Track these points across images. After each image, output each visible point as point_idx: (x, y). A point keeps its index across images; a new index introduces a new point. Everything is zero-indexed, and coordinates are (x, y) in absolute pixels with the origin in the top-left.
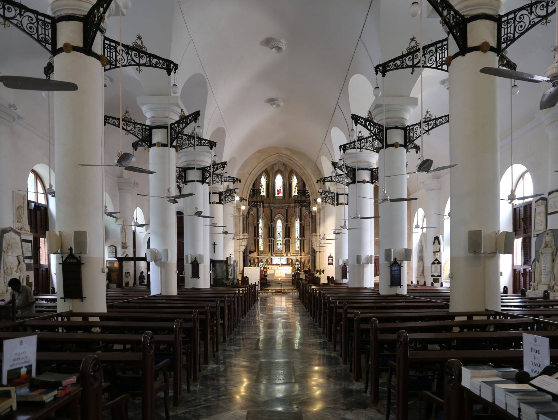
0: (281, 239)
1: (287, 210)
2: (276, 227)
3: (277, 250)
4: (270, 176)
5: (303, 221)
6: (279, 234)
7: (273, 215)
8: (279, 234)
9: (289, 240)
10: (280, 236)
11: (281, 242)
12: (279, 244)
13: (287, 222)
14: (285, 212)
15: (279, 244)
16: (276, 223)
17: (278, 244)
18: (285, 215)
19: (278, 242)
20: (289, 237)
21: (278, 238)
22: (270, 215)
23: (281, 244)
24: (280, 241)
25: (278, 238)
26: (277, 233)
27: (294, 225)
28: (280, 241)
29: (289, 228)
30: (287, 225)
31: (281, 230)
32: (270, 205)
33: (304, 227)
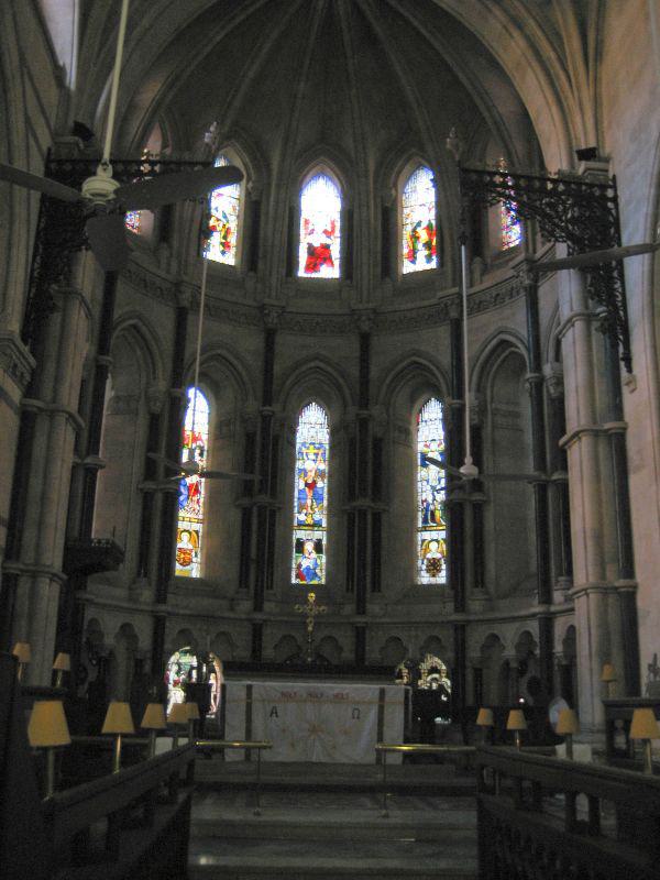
0: (321, 516)
1: (365, 340)
2: (293, 445)
3: (294, 581)
4: (268, 166)
6: (311, 486)
7: (277, 369)
8: (311, 486)
10: (317, 498)
11: (320, 535)
12: (309, 547)
15: (309, 547)
17: (300, 546)
19: (299, 534)
21: (302, 507)
22: (257, 364)
23: (318, 547)
24: (317, 525)
25: (302, 507)
26: (300, 484)
28: (317, 525)
31: (323, 466)
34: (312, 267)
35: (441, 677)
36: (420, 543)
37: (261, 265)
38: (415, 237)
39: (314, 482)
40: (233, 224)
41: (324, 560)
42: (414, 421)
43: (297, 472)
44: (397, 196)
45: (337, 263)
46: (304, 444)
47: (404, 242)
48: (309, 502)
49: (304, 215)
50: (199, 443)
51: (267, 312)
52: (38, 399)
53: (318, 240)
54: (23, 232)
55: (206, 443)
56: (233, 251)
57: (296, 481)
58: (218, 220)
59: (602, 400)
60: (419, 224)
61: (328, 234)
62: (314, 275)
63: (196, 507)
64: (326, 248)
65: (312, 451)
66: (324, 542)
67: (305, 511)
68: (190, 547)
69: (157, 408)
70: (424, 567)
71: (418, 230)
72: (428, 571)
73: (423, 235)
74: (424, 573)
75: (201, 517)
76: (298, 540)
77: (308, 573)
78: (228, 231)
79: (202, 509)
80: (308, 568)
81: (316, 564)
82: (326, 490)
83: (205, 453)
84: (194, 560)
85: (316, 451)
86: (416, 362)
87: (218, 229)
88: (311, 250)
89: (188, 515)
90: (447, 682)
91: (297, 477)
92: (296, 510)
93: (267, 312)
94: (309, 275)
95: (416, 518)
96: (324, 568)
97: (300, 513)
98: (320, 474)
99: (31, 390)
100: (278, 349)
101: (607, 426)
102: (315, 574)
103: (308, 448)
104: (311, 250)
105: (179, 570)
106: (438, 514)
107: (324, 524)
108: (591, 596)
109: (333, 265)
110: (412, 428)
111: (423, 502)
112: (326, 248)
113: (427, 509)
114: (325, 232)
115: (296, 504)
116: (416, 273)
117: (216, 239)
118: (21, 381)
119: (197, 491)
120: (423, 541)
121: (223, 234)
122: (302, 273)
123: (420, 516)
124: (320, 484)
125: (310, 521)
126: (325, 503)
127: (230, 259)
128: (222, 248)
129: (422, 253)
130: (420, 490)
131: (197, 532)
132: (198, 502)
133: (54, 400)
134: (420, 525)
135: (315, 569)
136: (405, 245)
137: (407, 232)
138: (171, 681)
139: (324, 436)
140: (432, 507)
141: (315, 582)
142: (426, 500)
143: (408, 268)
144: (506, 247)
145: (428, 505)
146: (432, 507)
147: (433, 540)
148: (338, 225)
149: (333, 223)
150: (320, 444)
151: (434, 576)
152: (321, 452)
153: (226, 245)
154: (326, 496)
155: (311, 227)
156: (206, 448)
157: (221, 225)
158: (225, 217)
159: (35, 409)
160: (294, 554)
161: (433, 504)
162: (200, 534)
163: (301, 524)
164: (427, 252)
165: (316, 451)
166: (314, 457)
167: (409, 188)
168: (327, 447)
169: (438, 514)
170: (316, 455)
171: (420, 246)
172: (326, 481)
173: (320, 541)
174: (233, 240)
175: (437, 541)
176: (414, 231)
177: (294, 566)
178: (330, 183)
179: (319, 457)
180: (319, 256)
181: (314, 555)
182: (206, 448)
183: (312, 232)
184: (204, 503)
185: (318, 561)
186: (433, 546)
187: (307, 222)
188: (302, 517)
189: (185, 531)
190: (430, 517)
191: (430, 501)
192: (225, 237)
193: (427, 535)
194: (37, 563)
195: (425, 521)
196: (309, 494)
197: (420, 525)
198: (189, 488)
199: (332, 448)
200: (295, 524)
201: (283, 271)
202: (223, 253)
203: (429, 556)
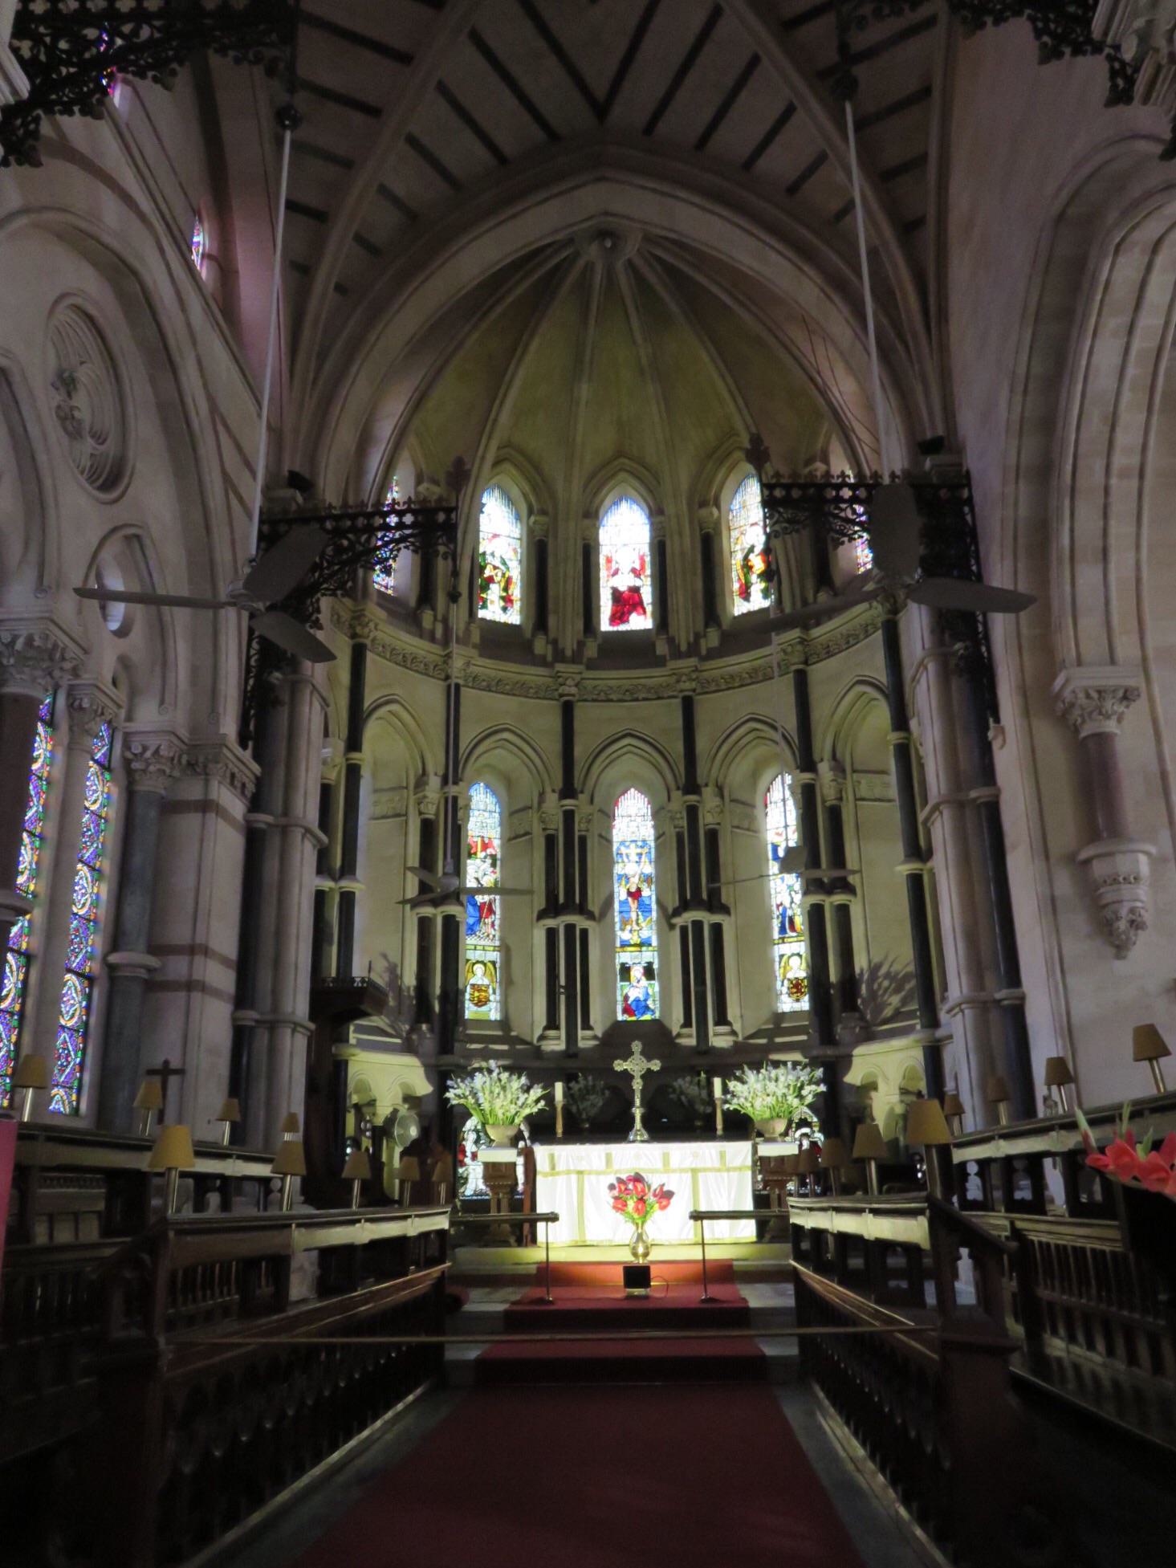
1: (688, 706)
3: (620, 1017)
6: (636, 895)
7: (578, 751)
8: (636, 895)
9: (717, 929)
10: (644, 909)
11: (650, 955)
12: (637, 972)
13: (691, 786)
14: (678, 722)
15: (637, 972)
16: (608, 816)
17: (625, 971)
18: (678, 748)
19: (624, 957)
20: (715, 904)
21: (625, 922)
22: (552, 747)
23: (649, 972)
24: (643, 944)
25: (625, 922)
26: (621, 893)
27: (752, 818)
28: (643, 944)
29: (713, 836)
30: (692, 812)
31: (649, 869)
32: (556, 677)
33: (835, 814)
34: (619, 616)
35: (813, 1132)
36: (777, 959)
37: (552, 621)
38: (747, 567)
39: (639, 890)
40: (515, 572)
41: (657, 989)
42: (759, 803)
43: (615, 878)
44: (719, 518)
45: (649, 609)
46: (622, 843)
47: (734, 575)
48: (633, 916)
49: (604, 552)
50: (489, 851)
53: (624, 582)
55: (498, 850)
56: (517, 605)
57: (616, 890)
58: (495, 568)
59: (967, 761)
60: (751, 550)
61: (637, 573)
62: (623, 627)
64: (635, 590)
65: (633, 851)
66: (656, 966)
67: (628, 927)
68: (486, 981)
69: (430, 812)
70: (785, 990)
71: (752, 557)
72: (790, 994)
73: (758, 564)
74: (785, 998)
75: (497, 943)
76: (623, 965)
77: (637, 1006)
78: (508, 581)
79: (498, 935)
80: (637, 1000)
81: (648, 994)
82: (654, 898)
83: (498, 863)
84: (492, 998)
85: (639, 851)
87: (497, 579)
88: (617, 595)
89: (482, 942)
90: (819, 1137)
91: (616, 886)
92: (617, 926)
94: (615, 629)
95: (769, 928)
96: (657, 998)
97: (622, 929)
98: (647, 879)
100: (578, 725)
101: (973, 794)
102: (647, 1008)
103: (628, 847)
104: (617, 595)
105: (470, 1011)
106: (799, 921)
107: (654, 943)
108: (966, 1011)
109: (645, 612)
110: (759, 811)
111: (778, 906)
112: (635, 590)
113: (783, 915)
114: (634, 571)
115: (617, 919)
116: (750, 614)
117: (494, 593)
119: (491, 911)
120: (781, 956)
121: (503, 584)
122: (605, 626)
123: (776, 924)
124: (646, 892)
125: (635, 940)
126: (654, 914)
127: (514, 617)
128: (502, 603)
129: (757, 587)
130: (773, 892)
131: (494, 963)
132: (493, 925)
134: (776, 935)
135: (646, 1000)
136: (735, 578)
137: (737, 561)
138: (468, 1154)
139: (647, 831)
140: (789, 913)
141: (647, 1017)
142: (781, 904)
143: (740, 608)
144: (862, 570)
145: (785, 910)
146: (789, 913)
147: (793, 955)
148: (648, 559)
149: (642, 559)
150: (644, 841)
151: (798, 1000)
152: (646, 850)
153: (507, 600)
154: (654, 906)
155: (614, 566)
156: (499, 856)
157: (500, 574)
158: (504, 563)
160: (619, 984)
161: (791, 907)
162: (498, 965)
163: (625, 945)
164: (763, 585)
165: (639, 851)
166: (637, 859)
167: (736, 505)
168: (653, 844)
169: (799, 921)
170: (640, 855)
171: (754, 578)
172: (653, 887)
173: (650, 964)
174: (516, 592)
175: (799, 955)
176: (746, 558)
177: (619, 998)
178: (635, 507)
179: (643, 856)
180: (626, 603)
181: (644, 982)
182: (499, 856)
183: (616, 573)
184: (500, 926)
185: (650, 992)
186: (795, 961)
187: (609, 561)
188: (625, 935)
189: (478, 962)
190: (787, 924)
191: (788, 905)
192: (506, 589)
193: (785, 949)
195: (783, 930)
196: (633, 905)
197: (776, 935)
198: (481, 908)
199: (657, 847)
200: (618, 944)
201: (580, 625)
202: (505, 609)
203: (790, 975)
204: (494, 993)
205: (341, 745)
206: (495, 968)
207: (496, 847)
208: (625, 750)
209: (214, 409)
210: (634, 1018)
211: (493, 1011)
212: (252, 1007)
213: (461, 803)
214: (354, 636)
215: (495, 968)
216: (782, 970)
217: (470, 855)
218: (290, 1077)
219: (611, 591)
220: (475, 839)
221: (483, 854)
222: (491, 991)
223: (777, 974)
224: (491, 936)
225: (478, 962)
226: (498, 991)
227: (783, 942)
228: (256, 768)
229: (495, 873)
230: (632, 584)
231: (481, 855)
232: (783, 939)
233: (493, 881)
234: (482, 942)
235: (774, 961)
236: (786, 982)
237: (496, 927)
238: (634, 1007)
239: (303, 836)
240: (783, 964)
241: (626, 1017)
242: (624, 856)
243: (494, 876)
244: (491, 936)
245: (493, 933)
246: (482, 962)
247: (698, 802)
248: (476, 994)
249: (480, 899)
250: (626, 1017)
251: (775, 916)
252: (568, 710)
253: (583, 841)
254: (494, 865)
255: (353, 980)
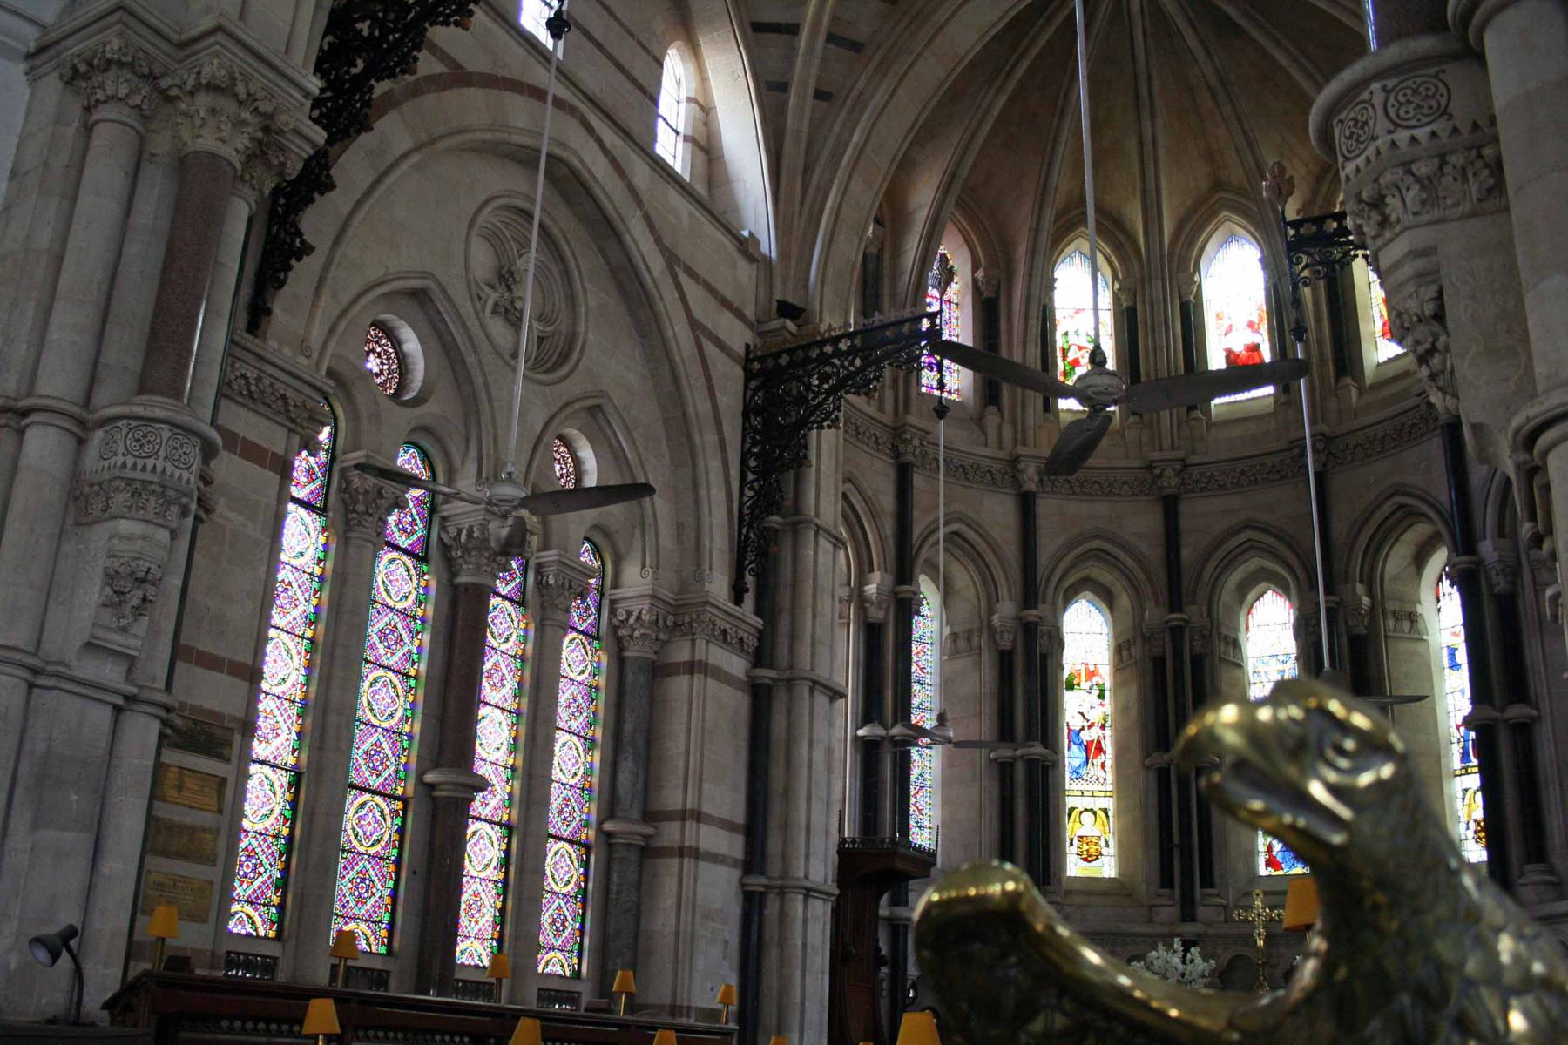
3: (1263, 871)
5: (1488, 549)
27: (1413, 618)
36: (1460, 795)
50: (1095, 679)
51: (1157, 471)
52: (771, 666)
54: (715, 465)
63: (1101, 774)
70: (1470, 834)
75: (1110, 787)
79: (1110, 777)
83: (1107, 694)
84: (1104, 851)
86: (1401, 506)
89: (1091, 787)
93: (1157, 471)
99: (761, 656)
100: (1184, 524)
118: (742, 650)
119: (1100, 750)
131: (1105, 811)
132: (1103, 766)
133: (791, 667)
156: (1108, 686)
159: (768, 681)
182: (1108, 686)
189: (1086, 810)
194: (785, 875)
204: (1107, 845)
205: (889, 579)
206: (1107, 816)
207: (1105, 675)
208: (1247, 545)
209: (671, 259)
210: (1280, 873)
211: (1106, 867)
212: (762, 873)
213: (1043, 628)
214: (896, 453)
215: (1107, 816)
216: (1466, 808)
217: (1070, 687)
218: (804, 945)
219: (1224, 354)
220: (1078, 667)
221: (1089, 684)
222: (1102, 843)
223: (1460, 814)
224: (1101, 780)
225: (1086, 810)
226: (1111, 843)
227: (1467, 773)
228: (758, 622)
229: (1101, 704)
230: (1249, 341)
231: (1085, 685)
232: (1466, 768)
233: (1102, 716)
234: (1091, 787)
235: (1453, 799)
236: (1472, 825)
237: (1108, 768)
238: (1279, 859)
239: (812, 691)
240: (1467, 801)
241: (1271, 871)
242: (1263, 674)
243: (1103, 709)
244: (1101, 780)
245: (1104, 775)
246: (1091, 810)
247: (1337, 604)
248: (1085, 847)
249: (1086, 736)
250: (1271, 871)
251: (1455, 740)
252: (1170, 507)
253: (1197, 661)
254: (1101, 696)
255: (883, 842)
